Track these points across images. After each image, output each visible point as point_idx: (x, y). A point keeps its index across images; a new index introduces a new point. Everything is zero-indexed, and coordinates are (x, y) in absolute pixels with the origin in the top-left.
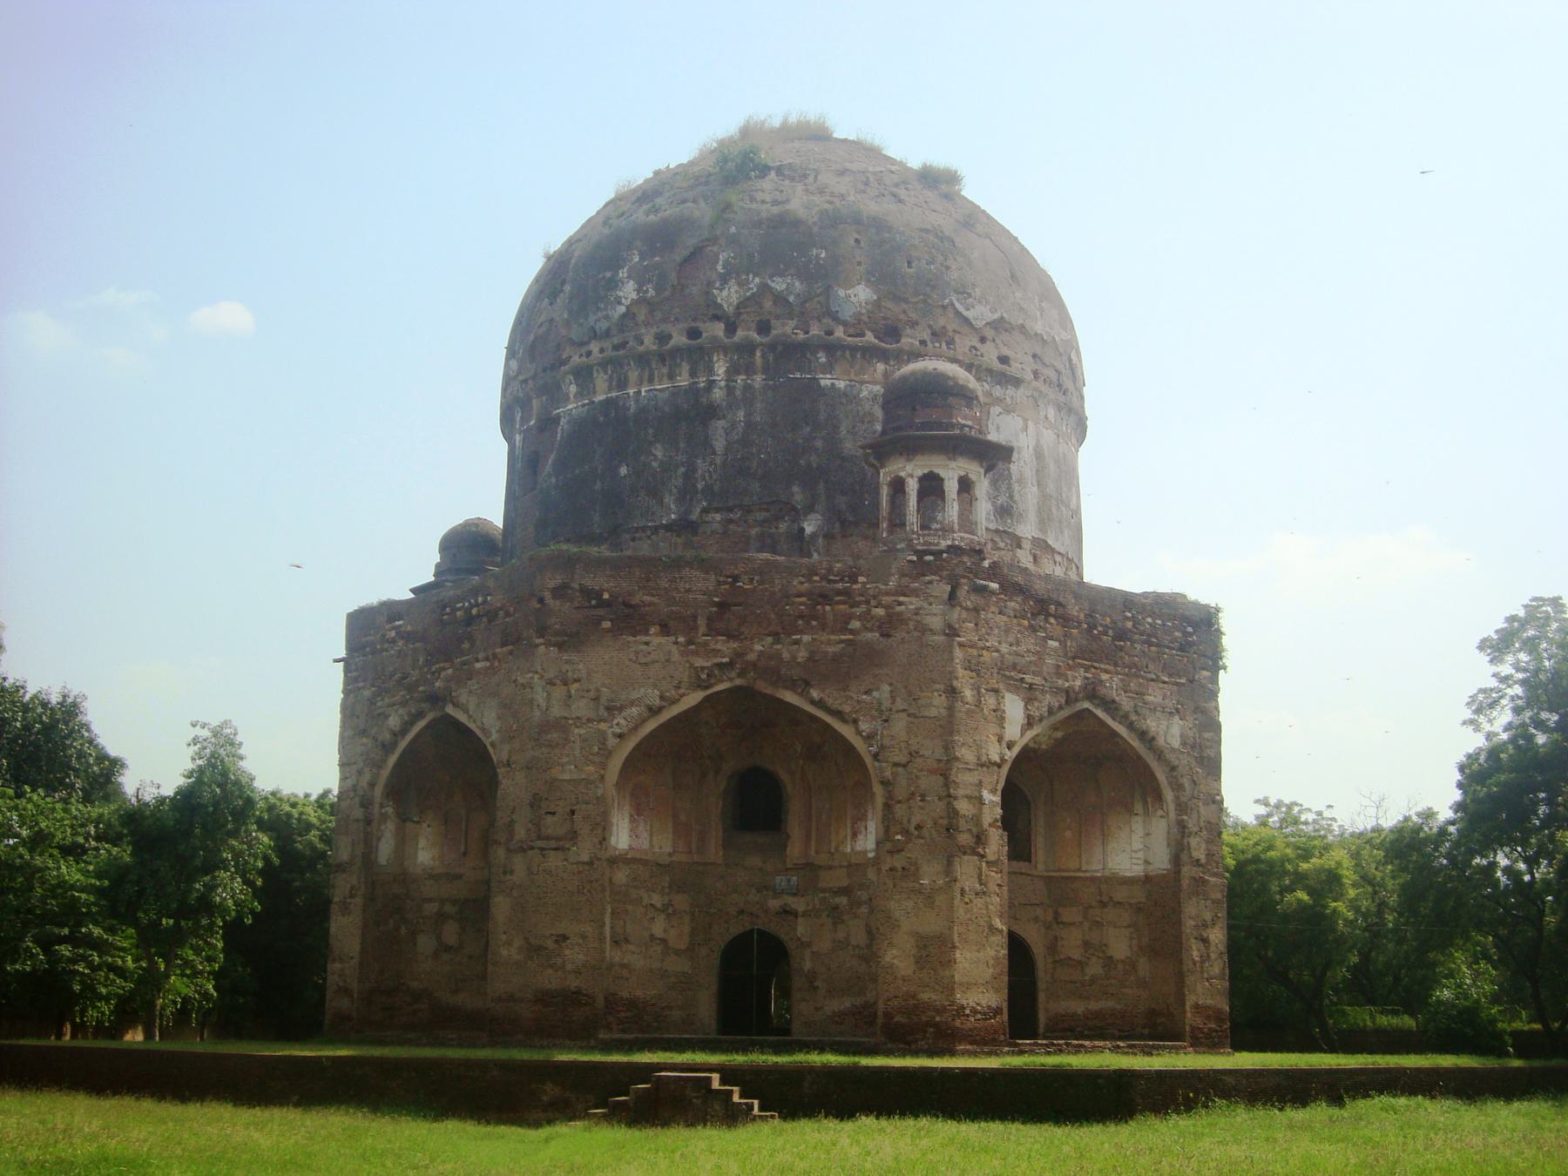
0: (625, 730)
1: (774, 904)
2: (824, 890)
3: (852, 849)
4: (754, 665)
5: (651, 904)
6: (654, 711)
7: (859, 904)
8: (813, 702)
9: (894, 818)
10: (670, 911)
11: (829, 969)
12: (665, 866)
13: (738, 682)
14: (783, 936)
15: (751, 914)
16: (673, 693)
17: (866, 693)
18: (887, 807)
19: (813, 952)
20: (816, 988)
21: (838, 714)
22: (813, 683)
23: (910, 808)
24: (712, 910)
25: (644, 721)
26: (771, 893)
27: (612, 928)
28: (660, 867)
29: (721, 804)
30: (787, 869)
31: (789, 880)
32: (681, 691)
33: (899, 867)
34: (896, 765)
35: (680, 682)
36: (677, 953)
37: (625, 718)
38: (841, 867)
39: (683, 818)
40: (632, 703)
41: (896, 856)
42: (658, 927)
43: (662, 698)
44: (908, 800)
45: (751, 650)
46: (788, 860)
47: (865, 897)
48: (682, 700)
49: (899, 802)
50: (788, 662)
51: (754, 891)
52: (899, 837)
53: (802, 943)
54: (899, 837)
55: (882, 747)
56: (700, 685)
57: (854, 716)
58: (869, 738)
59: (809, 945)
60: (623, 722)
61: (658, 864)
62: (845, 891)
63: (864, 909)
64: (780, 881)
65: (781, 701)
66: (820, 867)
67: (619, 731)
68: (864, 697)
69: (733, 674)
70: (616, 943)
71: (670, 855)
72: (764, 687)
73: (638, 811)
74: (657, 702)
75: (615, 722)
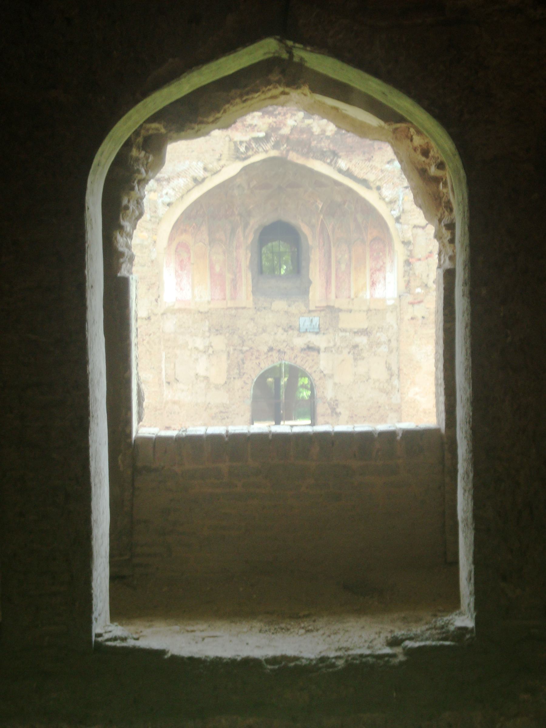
0: (173, 200)
1: (300, 342)
2: (345, 330)
3: (372, 296)
4: (287, 139)
5: (195, 348)
6: (197, 182)
7: (379, 344)
8: (340, 171)
9: (414, 274)
10: (210, 351)
11: (351, 398)
12: (207, 313)
13: (273, 153)
14: (307, 369)
15: (279, 351)
16: (214, 165)
17: (388, 162)
18: (408, 263)
19: (335, 384)
20: (338, 414)
21: (364, 182)
22: (341, 154)
23: (428, 265)
24: (245, 348)
25: (189, 191)
26: (296, 333)
27: (165, 371)
28: (205, 314)
29: (249, 255)
30: (310, 312)
31: (312, 321)
32: (222, 163)
33: (419, 316)
34: (415, 227)
35: (221, 155)
36: (217, 387)
37: (174, 189)
38: (360, 311)
39: (217, 269)
40: (179, 175)
41: (416, 307)
42: (202, 367)
43: (205, 169)
44: (427, 258)
45: (285, 125)
46: (311, 303)
47: (383, 338)
48: (224, 170)
49: (419, 260)
50: (318, 135)
51: (280, 330)
52: (419, 290)
53: (325, 375)
54: (419, 290)
55: (403, 211)
56: (238, 156)
57: (378, 184)
58: (392, 202)
59: (331, 376)
60: (171, 192)
61: (199, 312)
62: (365, 332)
63: (383, 349)
64: (304, 322)
65: (311, 171)
66: (340, 310)
67: (167, 200)
68: (387, 166)
69: (268, 147)
70: (169, 383)
71: (209, 302)
72: (294, 157)
73: (182, 265)
74: (201, 174)
75: (164, 192)
